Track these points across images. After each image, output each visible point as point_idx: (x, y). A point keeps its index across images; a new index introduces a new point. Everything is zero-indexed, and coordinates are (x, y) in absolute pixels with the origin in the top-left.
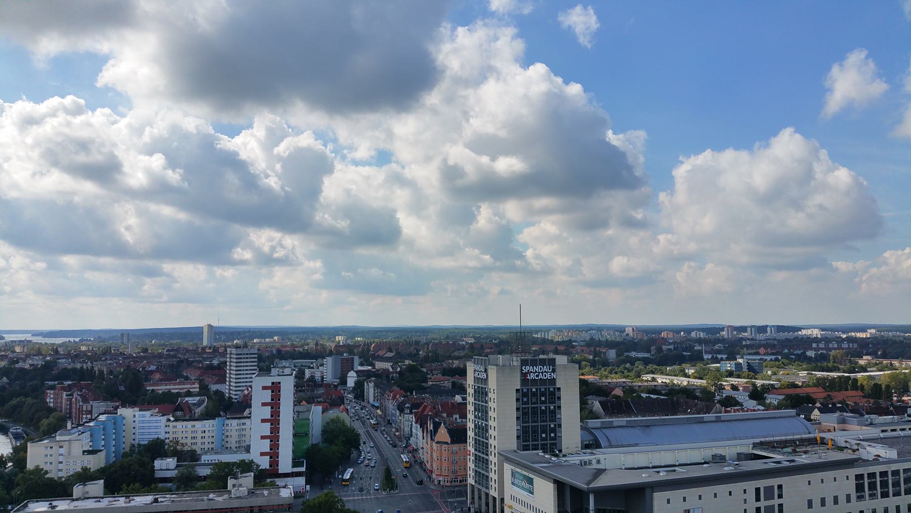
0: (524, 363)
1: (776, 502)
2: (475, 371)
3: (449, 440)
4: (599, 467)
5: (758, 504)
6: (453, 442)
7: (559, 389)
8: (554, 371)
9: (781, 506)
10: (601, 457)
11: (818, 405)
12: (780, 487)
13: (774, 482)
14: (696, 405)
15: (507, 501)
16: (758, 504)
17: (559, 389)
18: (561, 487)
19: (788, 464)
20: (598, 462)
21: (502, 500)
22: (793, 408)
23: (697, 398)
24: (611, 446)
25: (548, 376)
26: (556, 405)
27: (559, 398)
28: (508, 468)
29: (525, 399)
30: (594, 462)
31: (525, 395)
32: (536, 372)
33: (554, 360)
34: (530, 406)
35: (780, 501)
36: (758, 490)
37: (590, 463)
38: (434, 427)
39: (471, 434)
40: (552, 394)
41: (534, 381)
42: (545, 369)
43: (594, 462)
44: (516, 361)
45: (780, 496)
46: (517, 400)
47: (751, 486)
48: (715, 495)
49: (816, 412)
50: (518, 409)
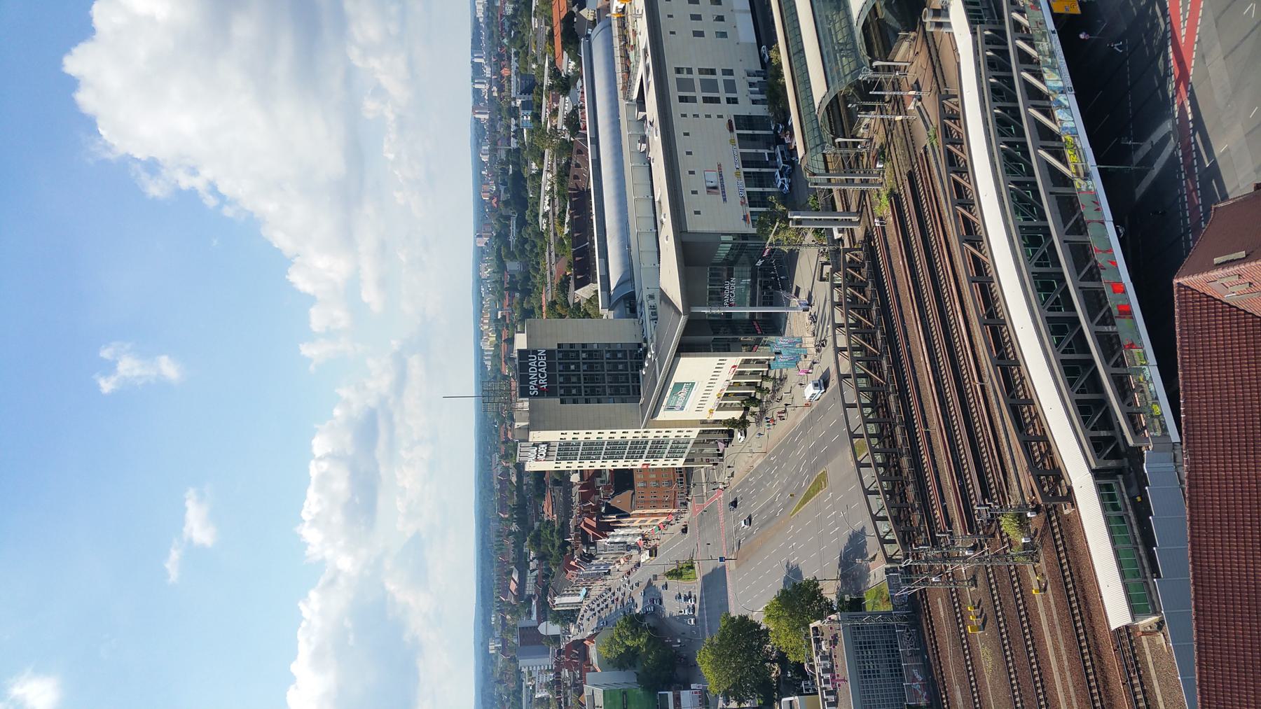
0: (524, 393)
1: (696, 76)
2: (537, 460)
3: (629, 492)
4: (657, 297)
5: (700, 99)
6: (632, 487)
7: (560, 346)
8: (535, 352)
9: (701, 71)
10: (646, 293)
11: (575, 9)
12: (679, 71)
13: (672, 77)
14: (578, 166)
15: (704, 416)
16: (700, 99)
17: (560, 346)
18: (687, 347)
19: (649, 60)
20: (652, 297)
21: (704, 422)
22: (578, 42)
23: (568, 164)
24: (632, 279)
25: (543, 360)
26: (580, 349)
27: (572, 345)
28: (663, 415)
29: (574, 391)
30: (651, 302)
31: (568, 392)
32: (538, 377)
33: (520, 351)
34: (582, 385)
35: (695, 71)
36: (682, 99)
37: (653, 308)
38: (613, 513)
39: (620, 464)
40: (566, 354)
41: (550, 379)
42: (533, 364)
43: (651, 302)
44: (524, 404)
45: (690, 71)
46: (575, 402)
47: (677, 108)
48: (689, 153)
49: (584, 12)
50: (587, 402)
